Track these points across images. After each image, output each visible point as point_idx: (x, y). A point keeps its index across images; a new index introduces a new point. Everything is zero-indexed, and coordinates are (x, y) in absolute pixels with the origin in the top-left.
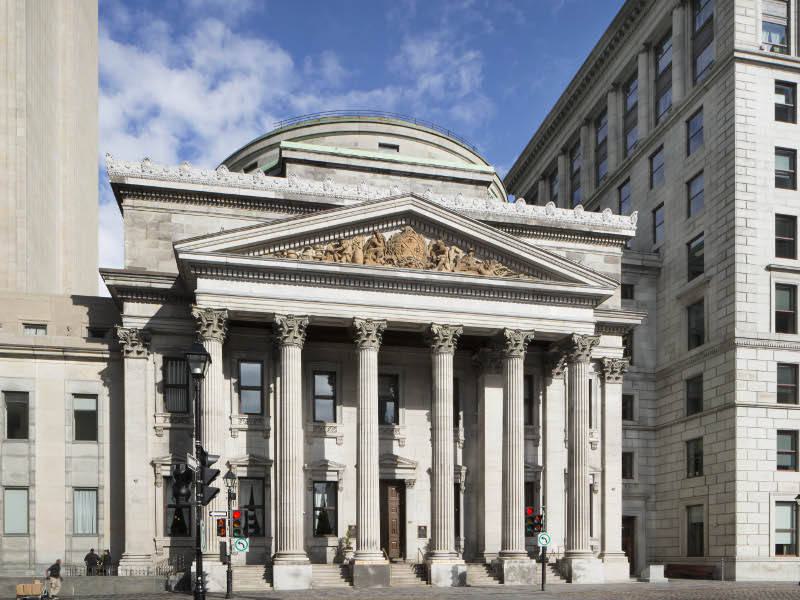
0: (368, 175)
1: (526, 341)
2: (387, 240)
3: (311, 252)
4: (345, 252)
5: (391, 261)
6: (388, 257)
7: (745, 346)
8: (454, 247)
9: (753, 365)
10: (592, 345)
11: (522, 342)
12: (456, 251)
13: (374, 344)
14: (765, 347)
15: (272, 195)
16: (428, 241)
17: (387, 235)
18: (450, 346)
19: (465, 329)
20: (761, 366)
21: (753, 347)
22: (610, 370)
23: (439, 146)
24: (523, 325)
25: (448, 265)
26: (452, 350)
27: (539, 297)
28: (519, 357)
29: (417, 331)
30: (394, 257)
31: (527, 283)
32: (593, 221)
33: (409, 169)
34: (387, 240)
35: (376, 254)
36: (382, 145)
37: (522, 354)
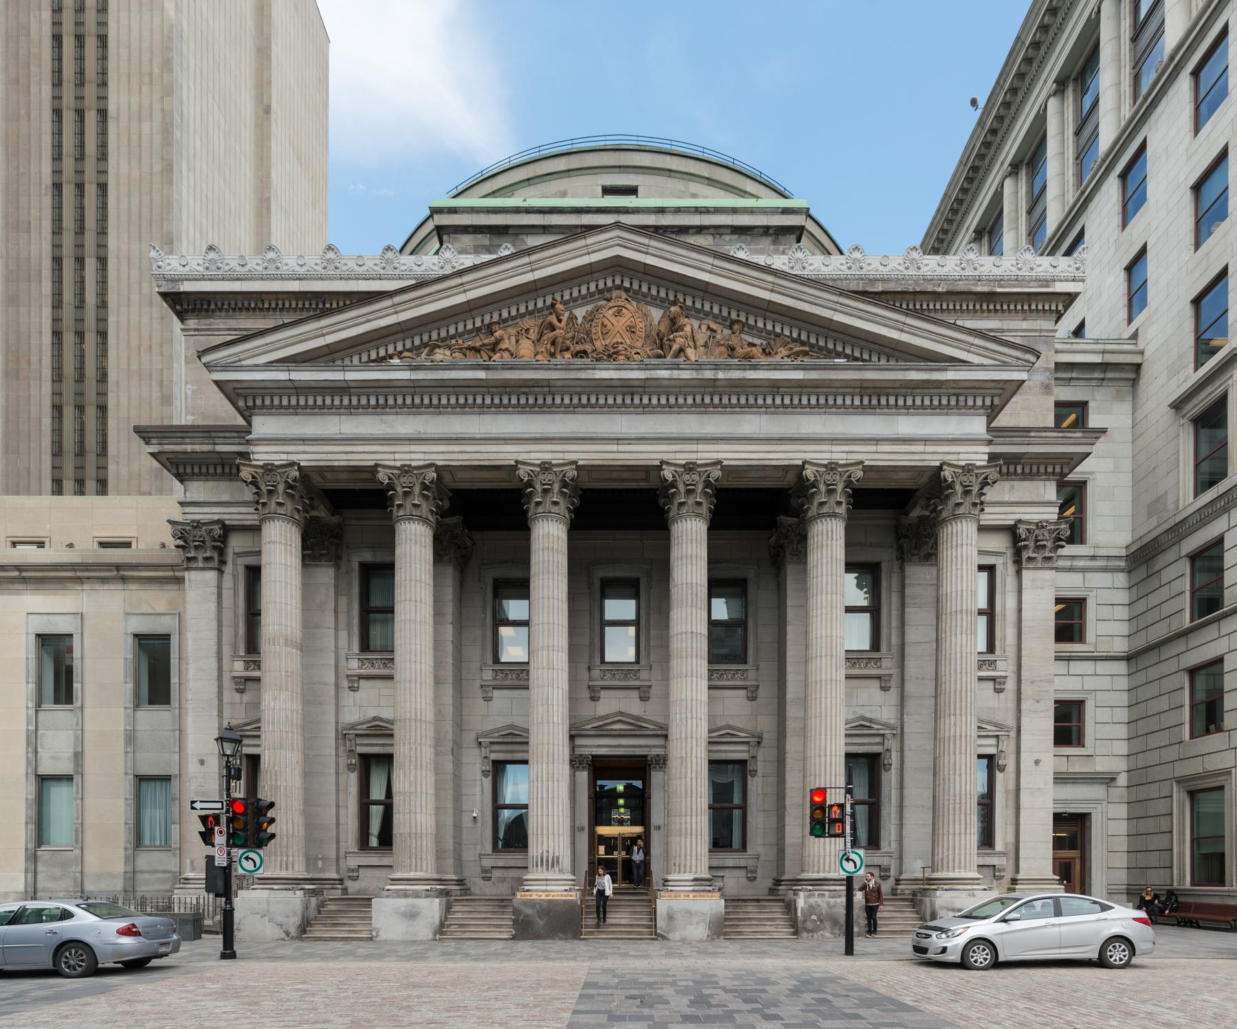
1: (849, 483)
2: (580, 320)
4: (503, 346)
6: (579, 347)
8: (705, 322)
10: (985, 483)
11: (840, 487)
12: (709, 328)
13: (555, 509)
16: (656, 314)
17: (580, 313)
18: (699, 504)
19: (729, 470)
22: (1031, 544)
24: (839, 454)
26: (704, 510)
28: (834, 515)
29: (643, 485)
30: (588, 347)
34: (580, 320)
35: (553, 343)
37: (842, 510)
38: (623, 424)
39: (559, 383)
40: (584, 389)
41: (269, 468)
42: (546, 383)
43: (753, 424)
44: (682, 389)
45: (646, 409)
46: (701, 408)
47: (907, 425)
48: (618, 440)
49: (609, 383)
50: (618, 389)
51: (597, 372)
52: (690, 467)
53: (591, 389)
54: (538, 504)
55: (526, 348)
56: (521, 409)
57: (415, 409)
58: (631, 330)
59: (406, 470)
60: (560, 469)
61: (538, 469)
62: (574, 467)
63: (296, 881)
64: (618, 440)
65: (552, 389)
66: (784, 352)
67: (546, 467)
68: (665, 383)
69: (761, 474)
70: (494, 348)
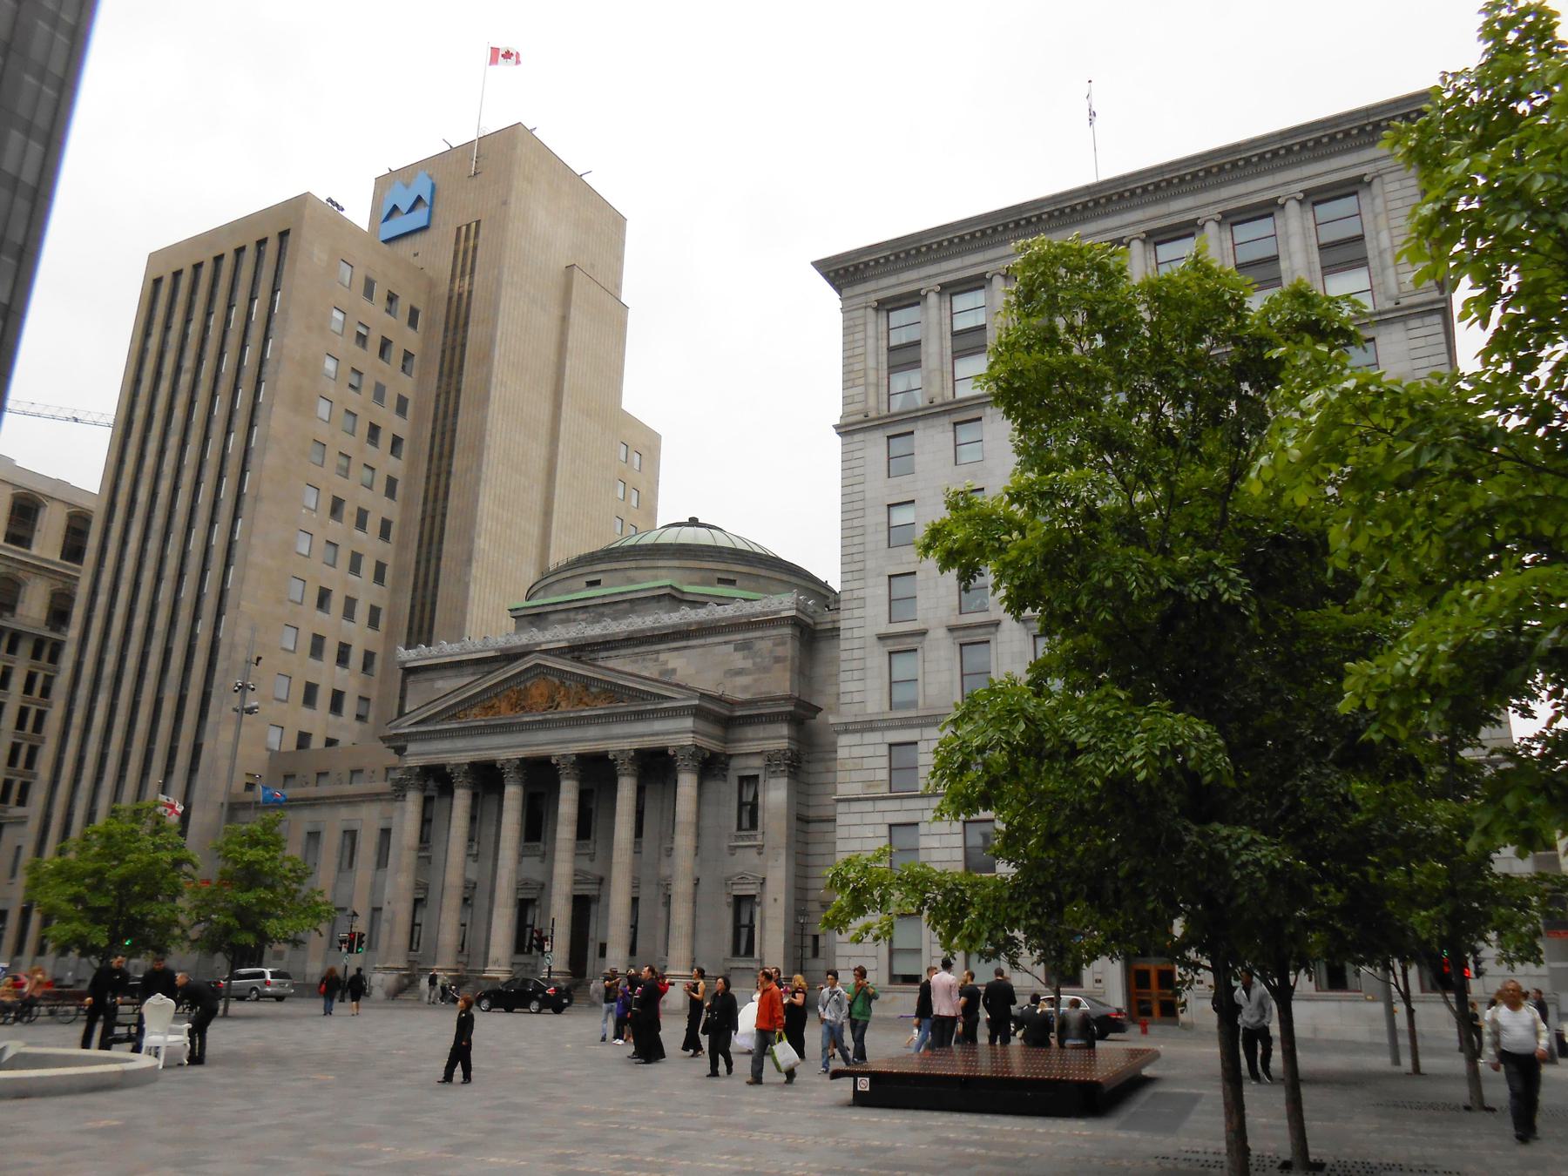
0: (572, 615)
3: (474, 711)
5: (523, 708)
6: (523, 703)
7: (846, 731)
9: (856, 752)
14: (872, 730)
15: (492, 654)
17: (528, 684)
20: (868, 751)
21: (855, 731)
23: (637, 568)
24: (626, 745)
25: (563, 704)
27: (640, 716)
31: (622, 707)
32: (753, 611)
33: (600, 601)
36: (591, 584)
38: (542, 736)
41: (410, 768)
43: (593, 731)
46: (569, 726)
47: (658, 726)
52: (564, 756)
55: (504, 705)
56: (502, 733)
57: (464, 736)
58: (541, 695)
59: (458, 765)
63: (398, 969)
66: (603, 696)
67: (508, 760)
70: (492, 707)
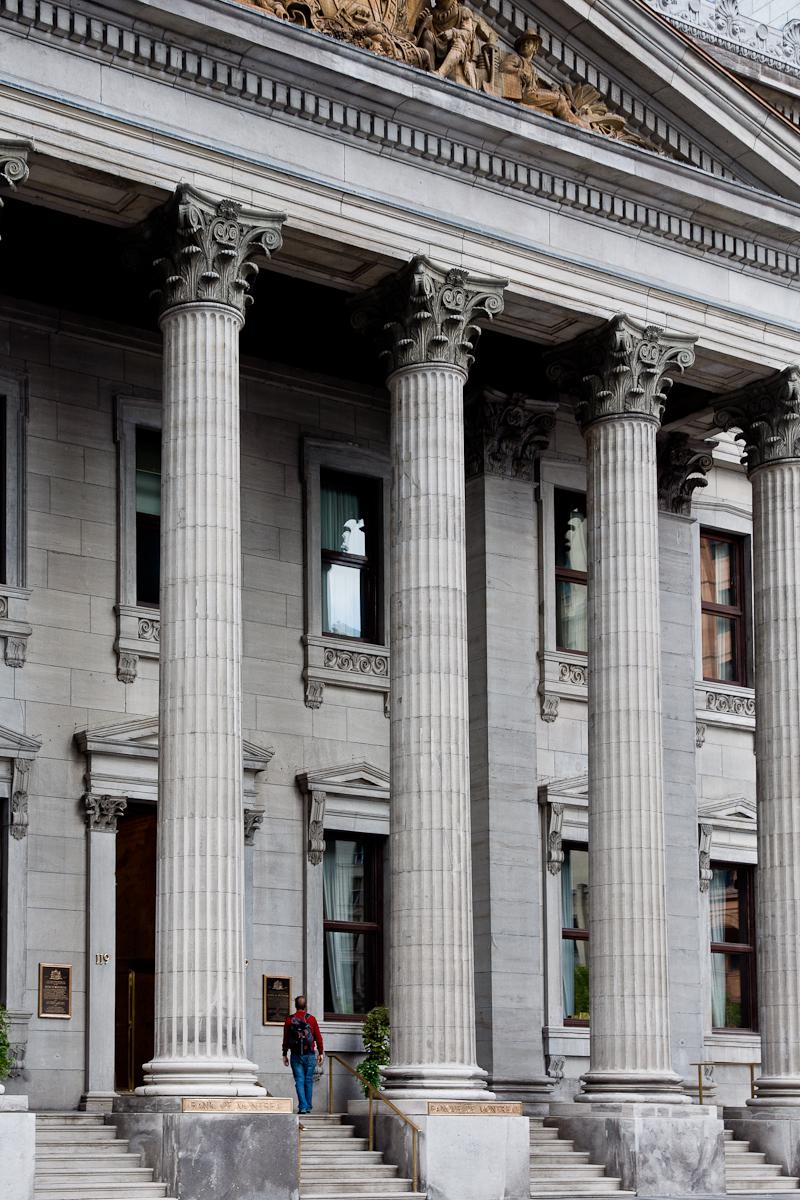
39: (265, 56)
40: (298, 80)
42: (241, 48)
44: (451, 133)
45: (388, 148)
48: (344, 195)
49: (344, 84)
50: (353, 100)
51: (337, 58)
53: (310, 85)
54: (208, 281)
60: (251, 223)
61: (212, 212)
62: (278, 226)
64: (344, 195)
65: (246, 62)
68: (433, 113)
69: (530, 314)
